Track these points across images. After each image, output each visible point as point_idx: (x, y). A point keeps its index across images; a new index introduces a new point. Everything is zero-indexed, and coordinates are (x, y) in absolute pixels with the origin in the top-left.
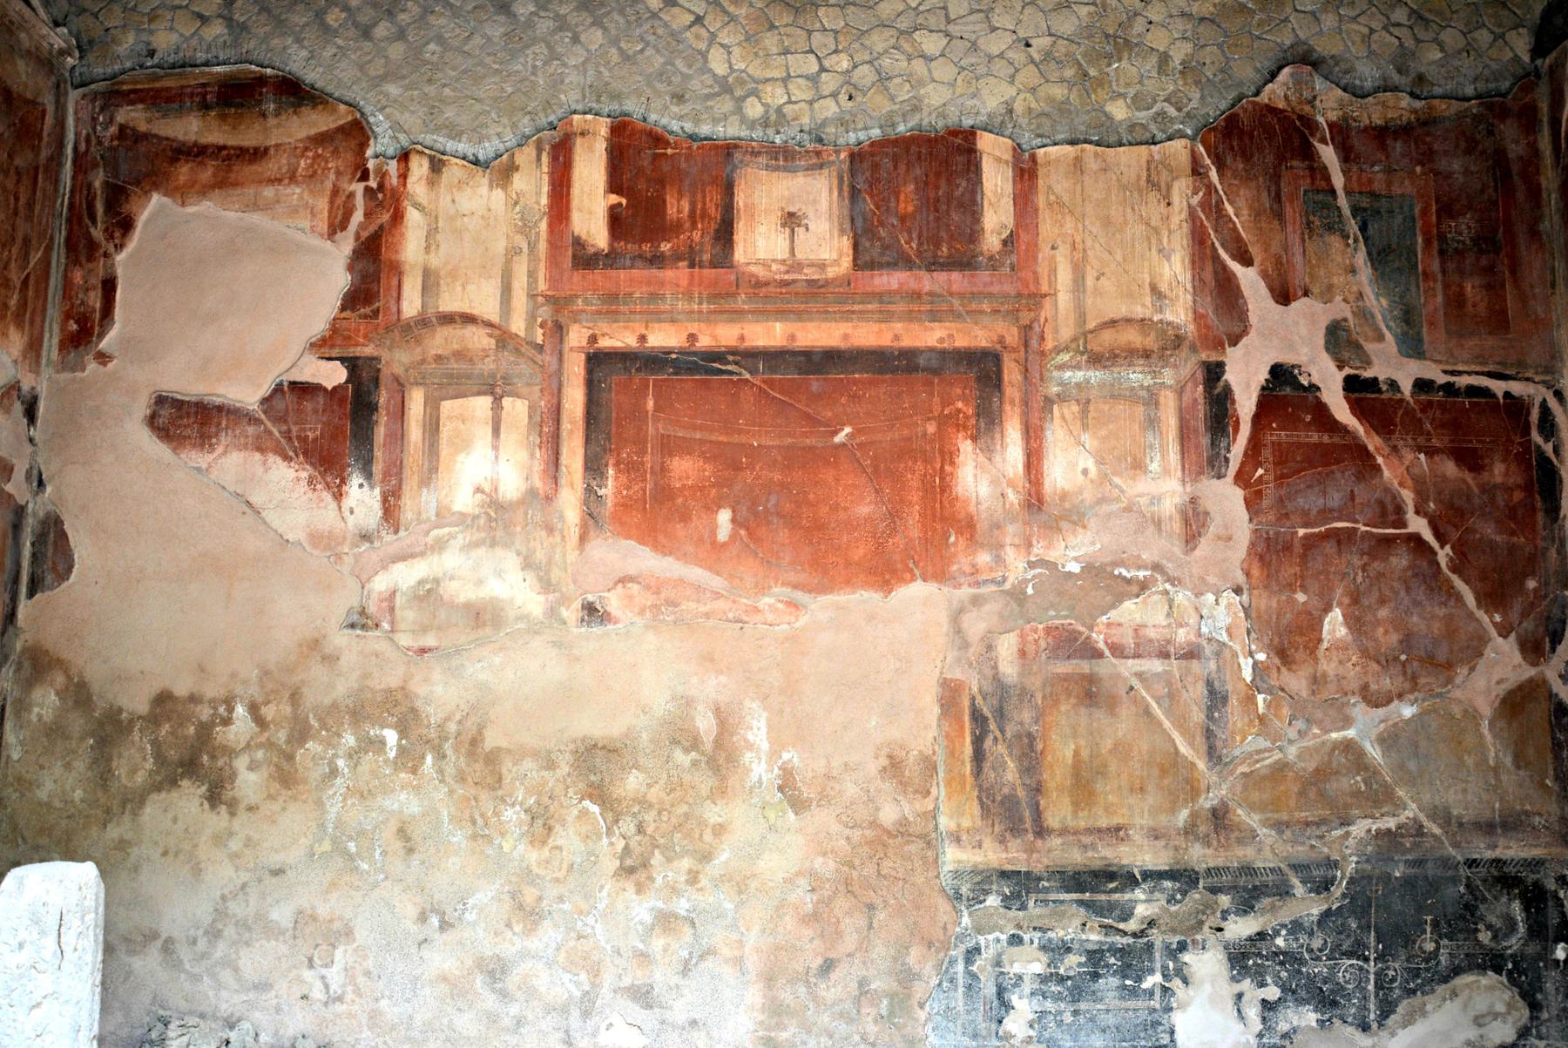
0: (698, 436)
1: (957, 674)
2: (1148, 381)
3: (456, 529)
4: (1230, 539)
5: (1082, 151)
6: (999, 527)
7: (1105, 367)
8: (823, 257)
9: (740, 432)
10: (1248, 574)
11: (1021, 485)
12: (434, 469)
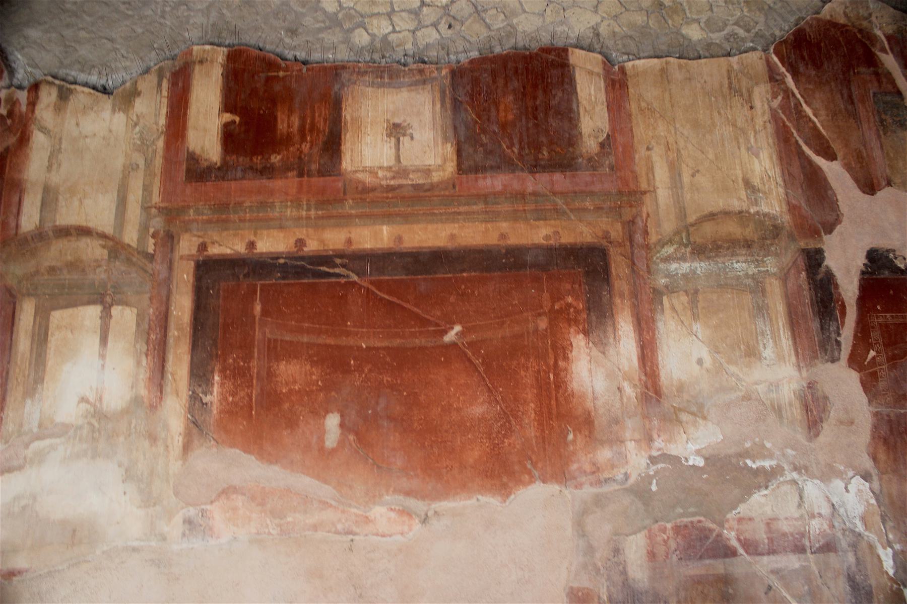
0: (305, 339)
1: (584, 582)
2: (752, 270)
3: (58, 440)
4: (852, 423)
5: (667, 63)
6: (617, 422)
7: (709, 258)
8: (427, 163)
9: (348, 334)
10: (875, 459)
11: (637, 378)
12: (39, 380)
